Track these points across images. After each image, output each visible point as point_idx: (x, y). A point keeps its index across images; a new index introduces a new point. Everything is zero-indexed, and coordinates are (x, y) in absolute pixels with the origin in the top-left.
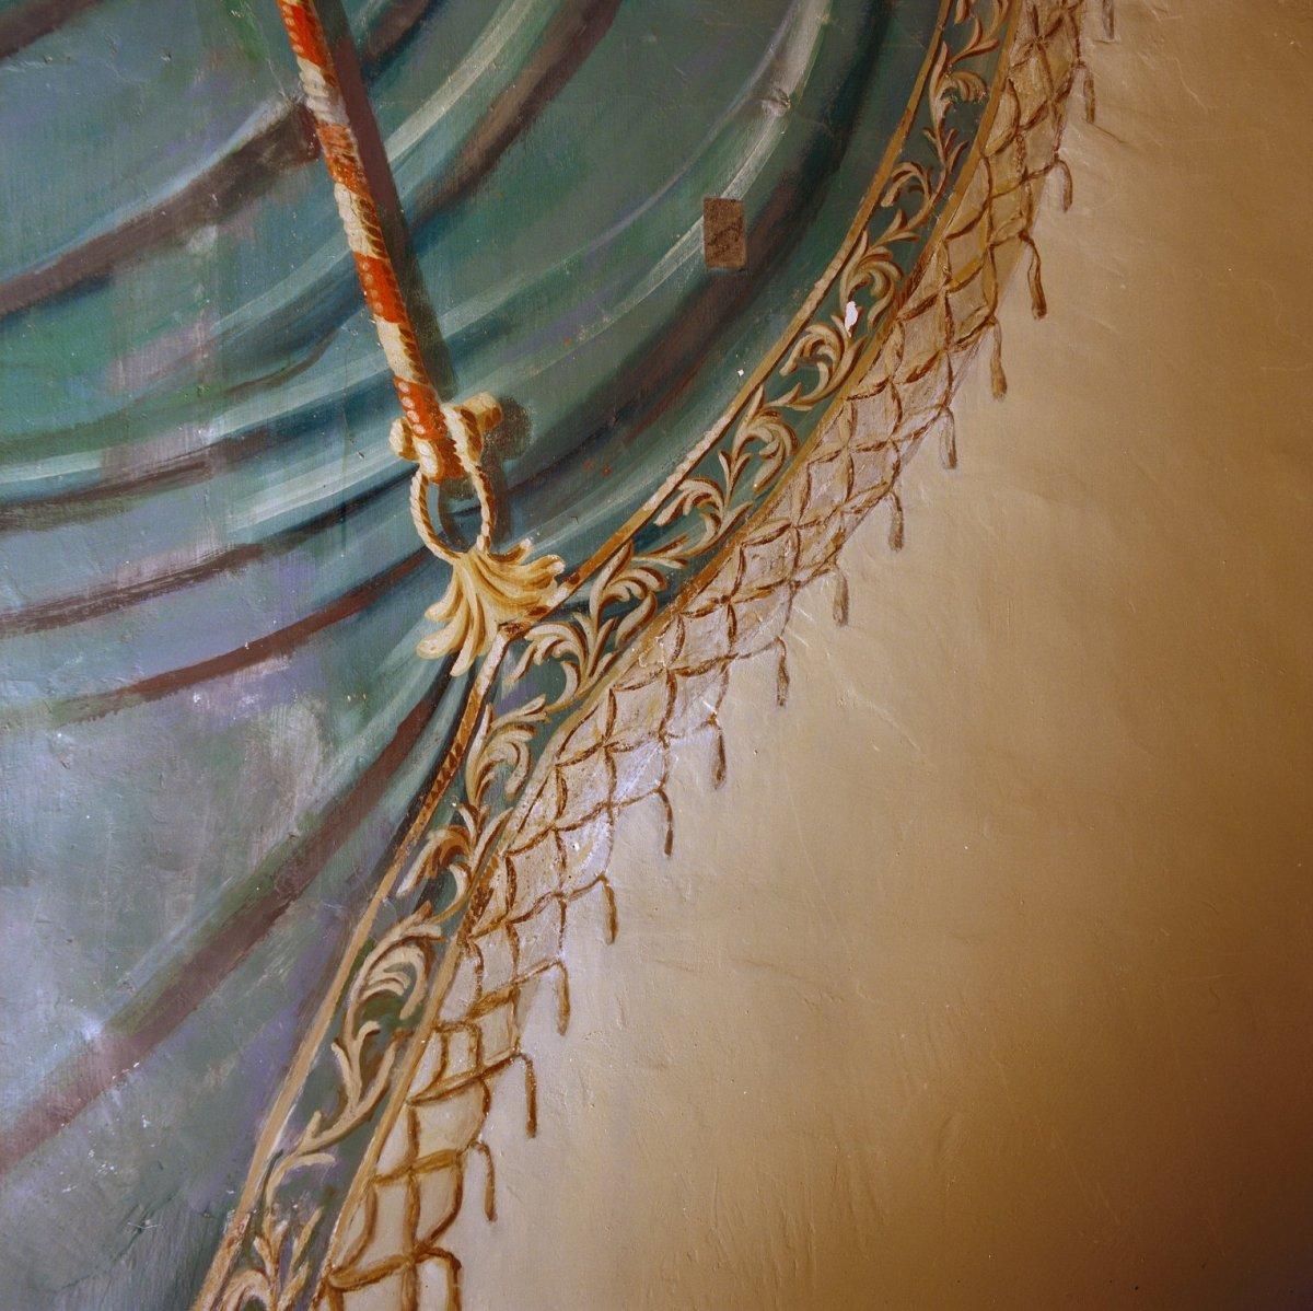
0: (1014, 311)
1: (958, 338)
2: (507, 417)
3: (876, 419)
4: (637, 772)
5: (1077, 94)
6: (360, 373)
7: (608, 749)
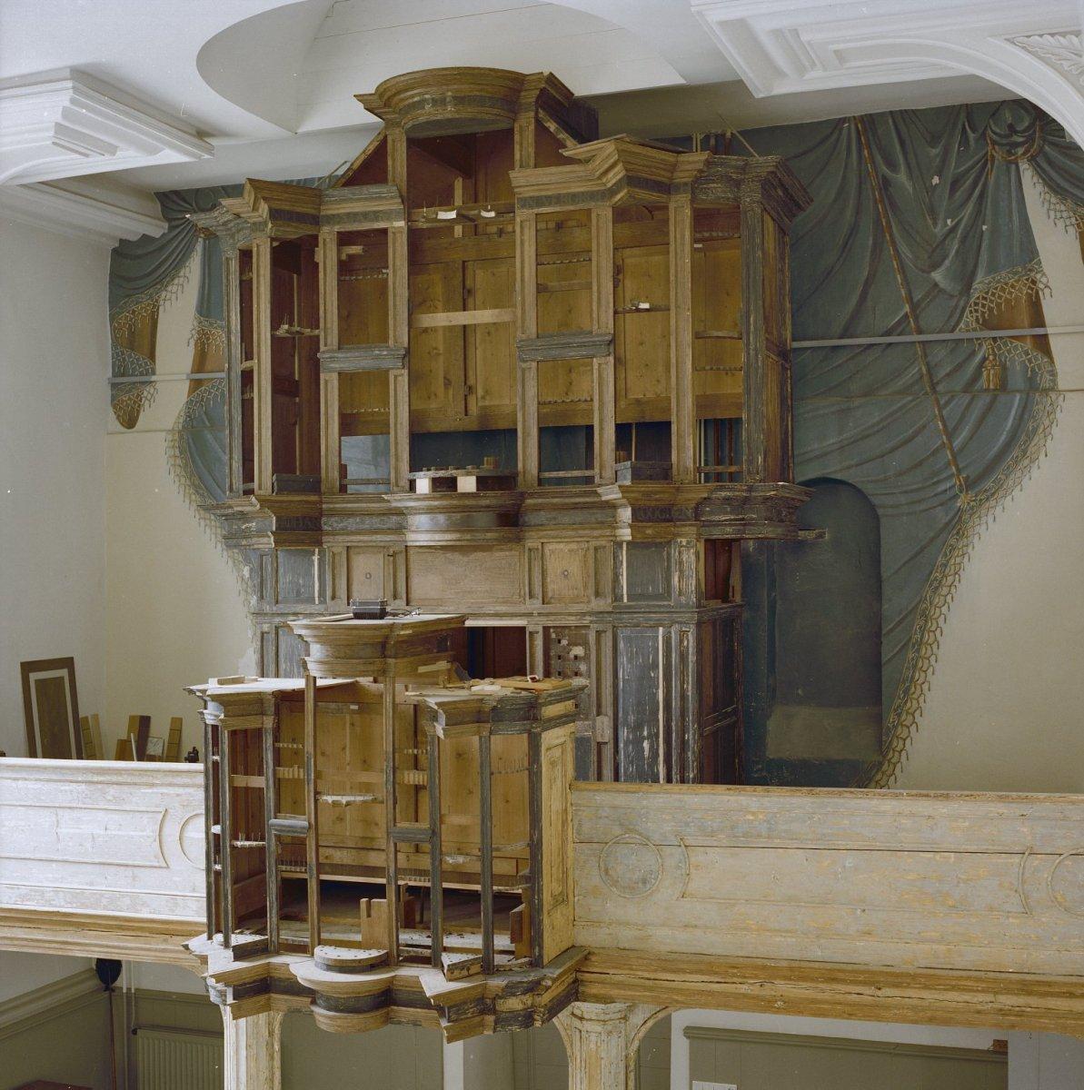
0: (1042, 457)
1: (1032, 461)
2: (968, 477)
3: (1019, 474)
4: (984, 520)
5: (1055, 423)
6: (950, 473)
7: (980, 517)
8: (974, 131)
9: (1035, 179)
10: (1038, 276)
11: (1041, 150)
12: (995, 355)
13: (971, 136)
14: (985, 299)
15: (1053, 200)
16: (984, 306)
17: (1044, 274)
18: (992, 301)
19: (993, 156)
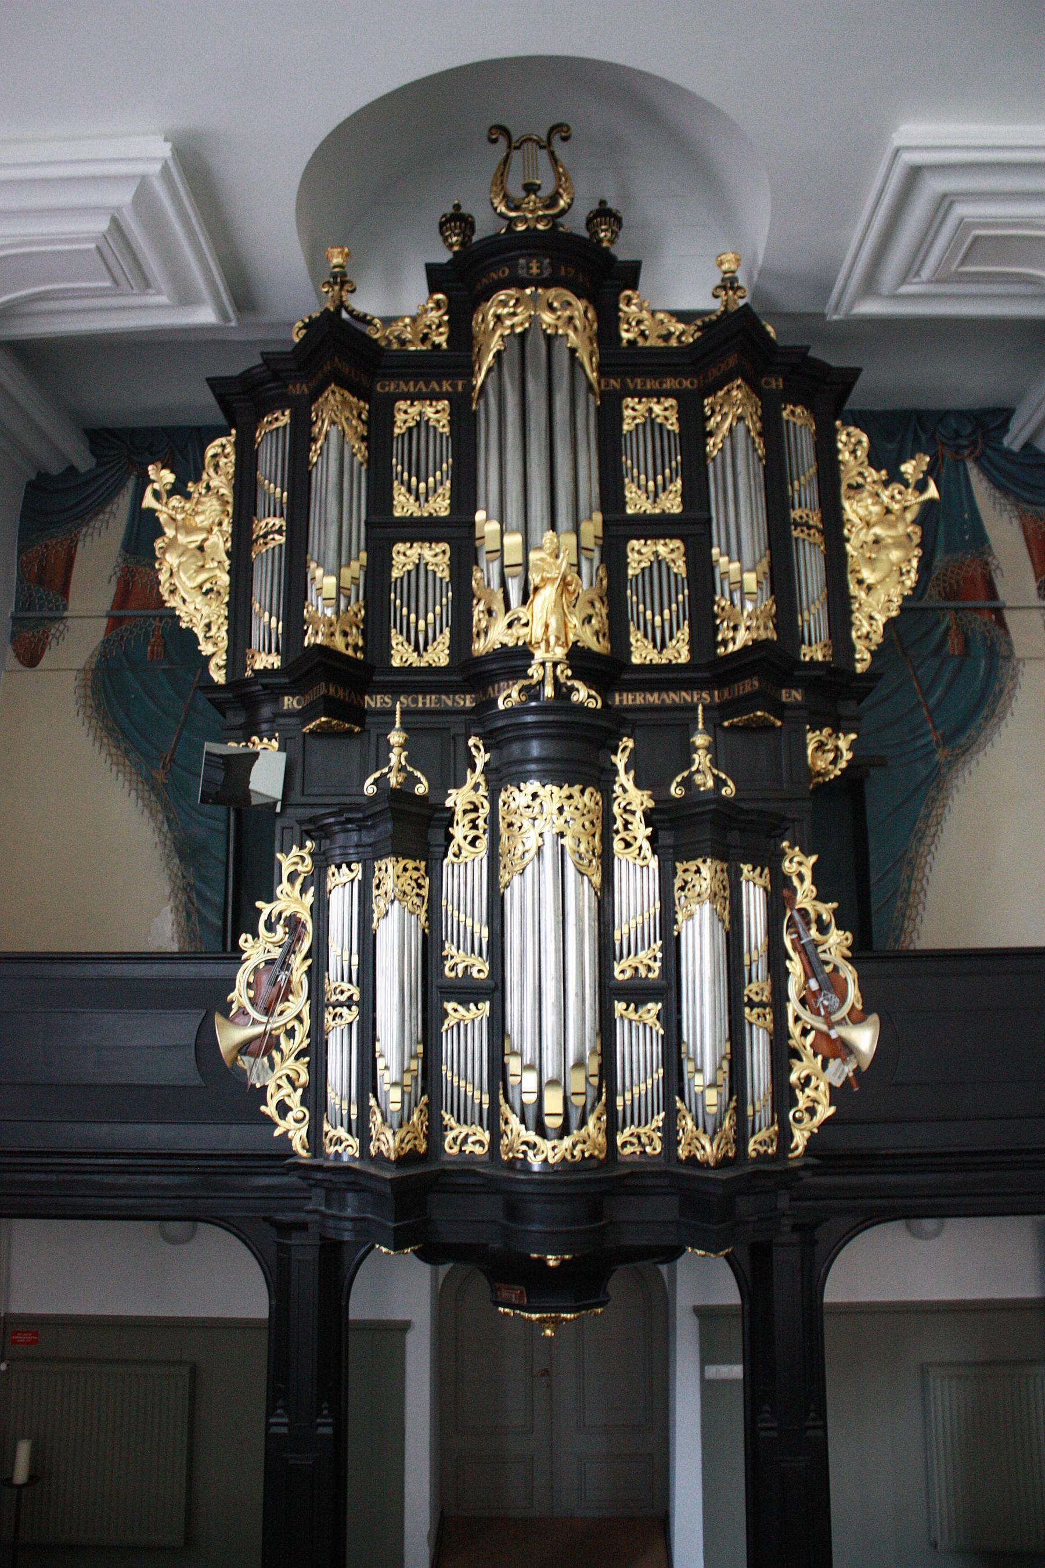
8: (924, 431)
9: (981, 476)
10: (990, 559)
11: (983, 453)
12: (958, 626)
13: (923, 437)
14: (945, 575)
15: (997, 495)
16: (944, 581)
17: (994, 557)
18: (951, 578)
19: (943, 456)
